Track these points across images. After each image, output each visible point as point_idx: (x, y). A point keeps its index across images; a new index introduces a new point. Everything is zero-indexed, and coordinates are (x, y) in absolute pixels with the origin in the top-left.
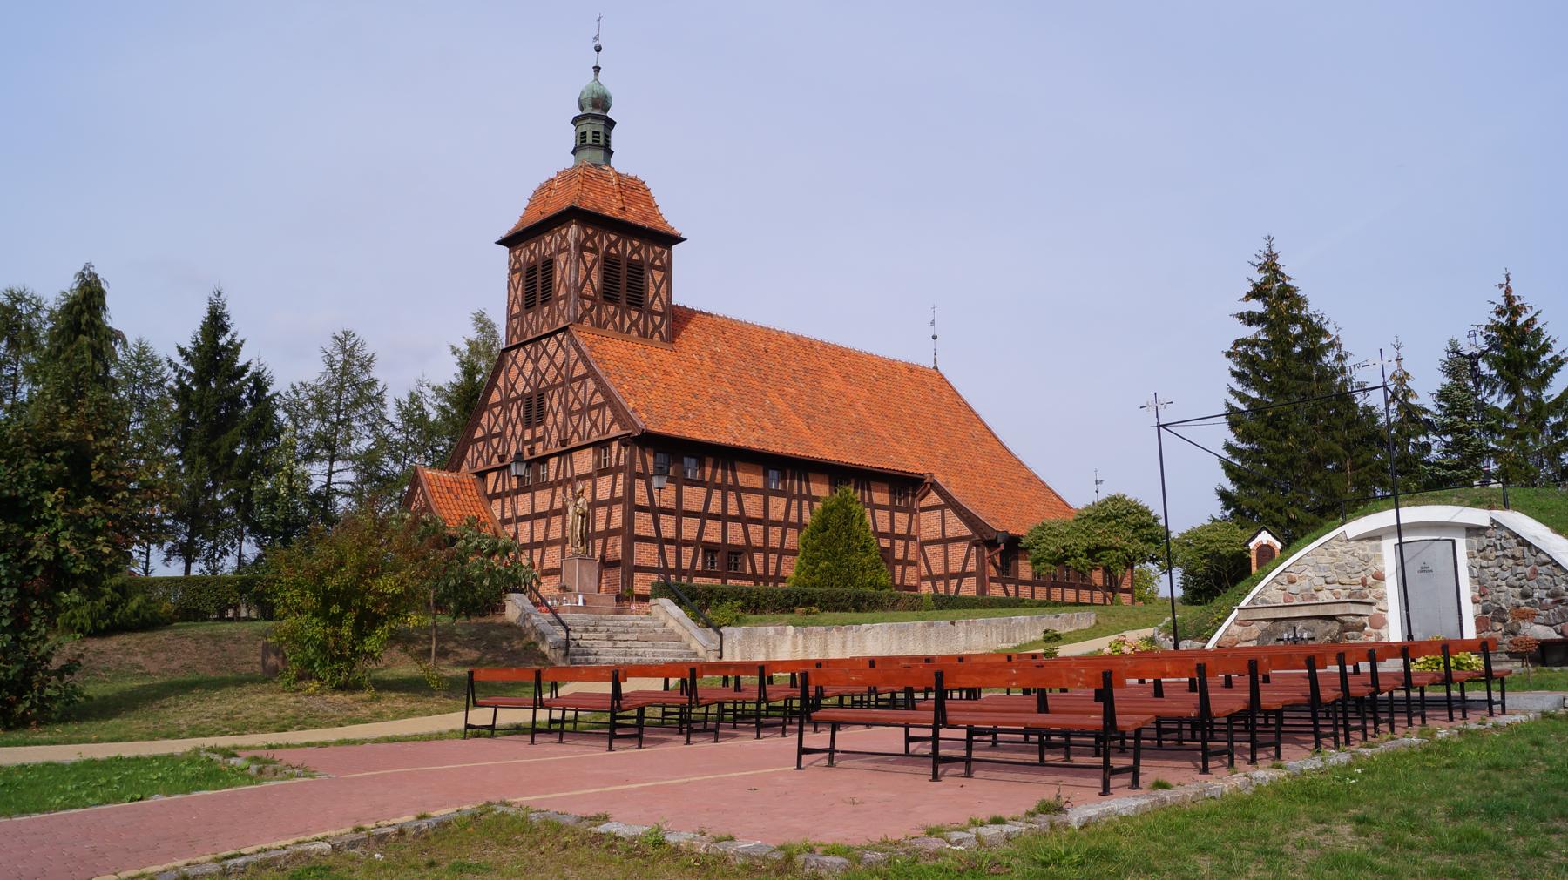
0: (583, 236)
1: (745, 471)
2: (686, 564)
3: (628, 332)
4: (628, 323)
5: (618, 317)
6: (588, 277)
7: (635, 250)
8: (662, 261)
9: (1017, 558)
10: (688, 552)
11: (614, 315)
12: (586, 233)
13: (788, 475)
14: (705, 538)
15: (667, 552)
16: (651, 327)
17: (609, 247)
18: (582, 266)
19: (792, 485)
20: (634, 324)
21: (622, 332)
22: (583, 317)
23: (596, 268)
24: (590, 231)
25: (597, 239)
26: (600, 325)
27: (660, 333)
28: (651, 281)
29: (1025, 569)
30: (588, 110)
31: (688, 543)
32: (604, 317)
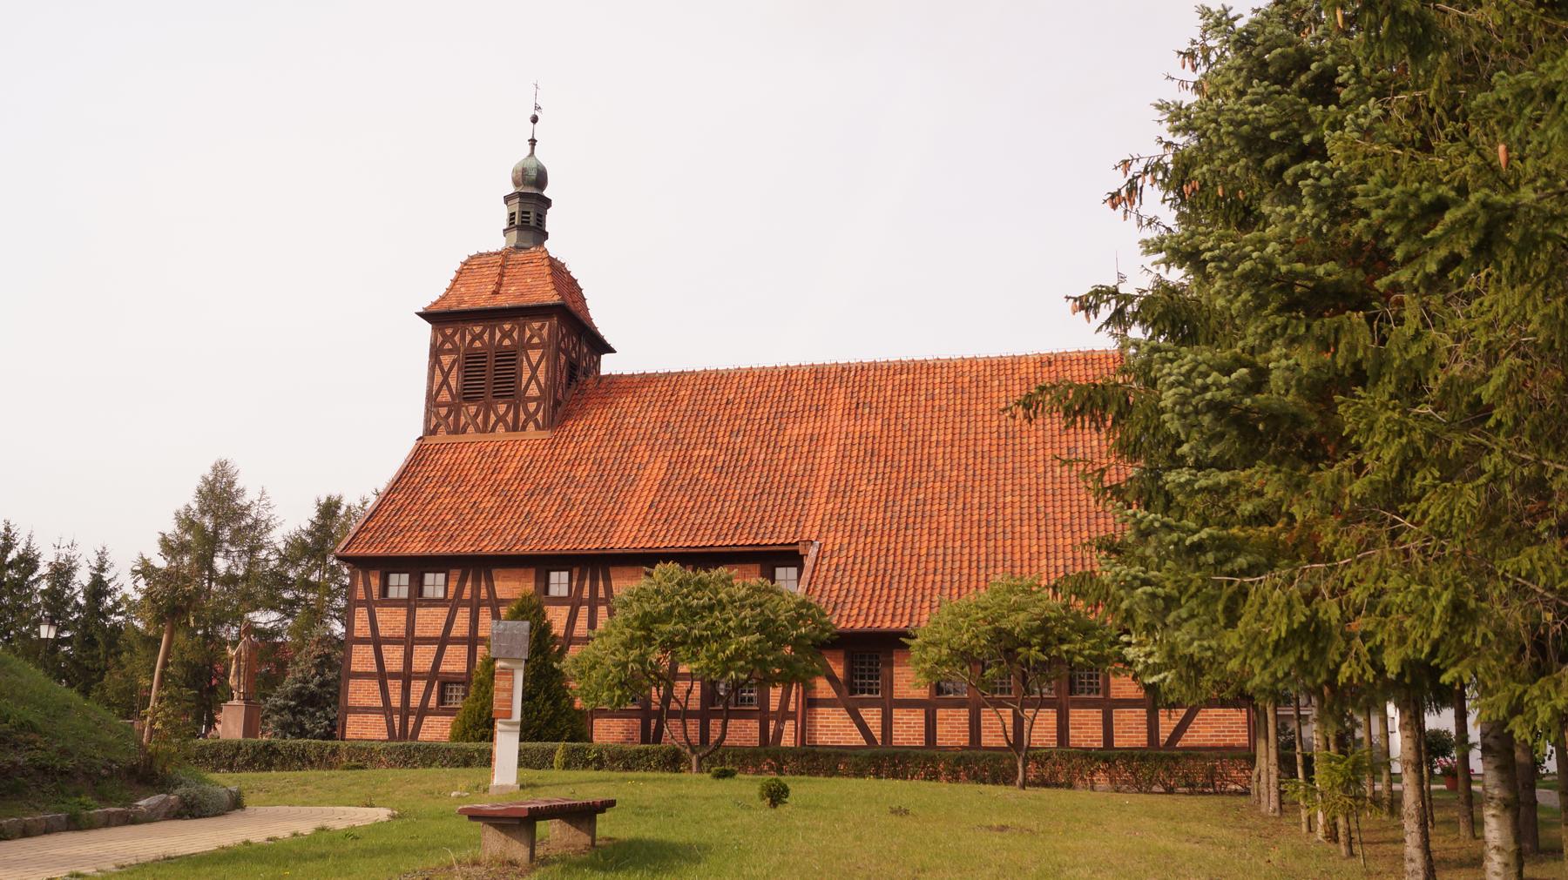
0: (440, 339)
1: (506, 578)
2: (415, 701)
3: (493, 430)
4: (493, 418)
5: (481, 417)
6: (445, 382)
7: (505, 335)
8: (540, 337)
9: (890, 664)
10: (418, 687)
11: (476, 415)
12: (444, 335)
13: (575, 577)
14: (443, 668)
15: (391, 689)
16: (522, 417)
17: (472, 341)
18: (438, 371)
19: (580, 588)
20: (501, 419)
21: (484, 431)
22: (437, 426)
23: (456, 368)
24: (449, 331)
25: (457, 338)
26: (457, 430)
27: (536, 422)
28: (525, 363)
29: (908, 680)
30: (521, 189)
31: (420, 676)
32: (463, 420)
